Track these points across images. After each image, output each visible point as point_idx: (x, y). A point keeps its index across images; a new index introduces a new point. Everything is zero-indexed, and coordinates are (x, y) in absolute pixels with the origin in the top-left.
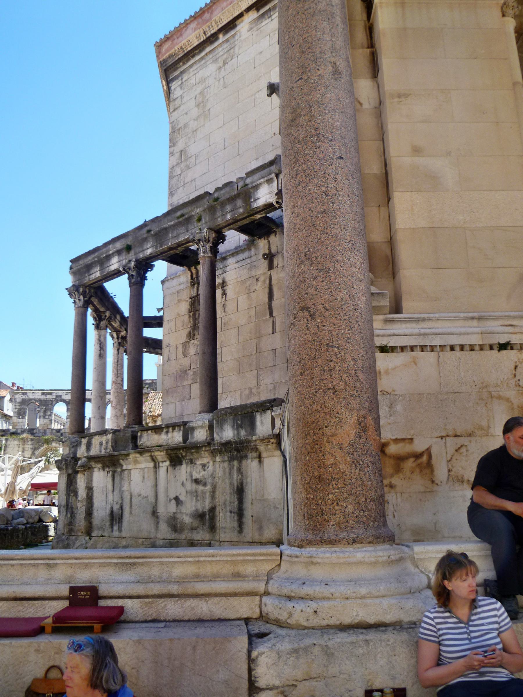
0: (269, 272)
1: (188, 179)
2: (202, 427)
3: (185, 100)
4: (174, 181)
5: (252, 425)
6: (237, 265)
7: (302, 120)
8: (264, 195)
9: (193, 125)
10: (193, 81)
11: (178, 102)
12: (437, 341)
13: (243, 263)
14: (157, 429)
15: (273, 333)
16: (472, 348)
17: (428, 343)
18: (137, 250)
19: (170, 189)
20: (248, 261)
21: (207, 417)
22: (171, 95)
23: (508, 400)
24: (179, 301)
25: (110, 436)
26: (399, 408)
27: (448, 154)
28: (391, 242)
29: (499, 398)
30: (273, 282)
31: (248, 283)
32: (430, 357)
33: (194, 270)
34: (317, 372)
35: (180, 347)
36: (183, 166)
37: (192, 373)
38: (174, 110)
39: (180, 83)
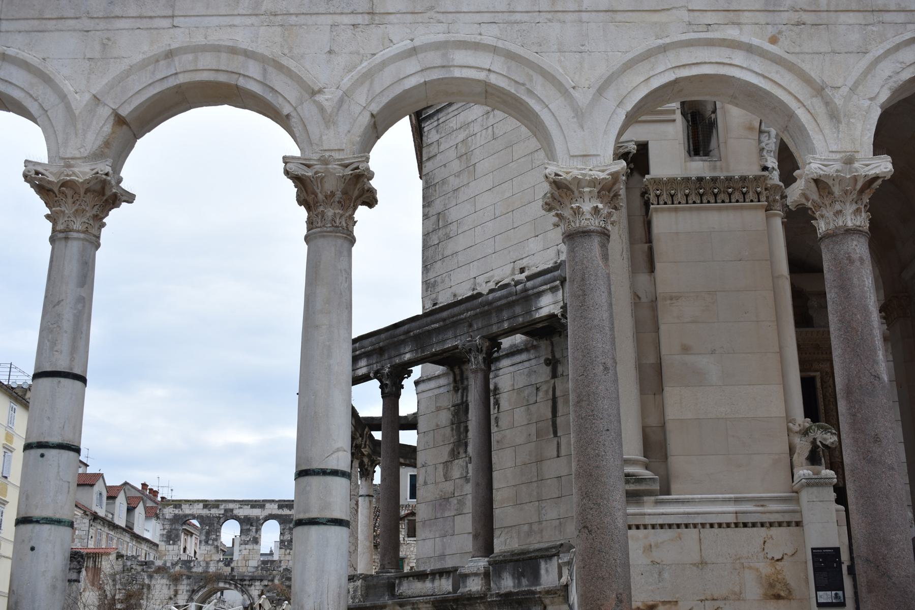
0: (553, 381)
1: (448, 252)
2: (476, 574)
3: (442, 148)
4: (430, 252)
5: (535, 577)
6: (512, 369)
7: (584, 404)
8: (548, 305)
9: (454, 182)
10: (454, 123)
11: (433, 150)
12: (699, 520)
13: (520, 366)
14: (421, 576)
15: (558, 456)
16: (728, 525)
17: (691, 521)
18: (393, 353)
19: (424, 262)
20: (527, 364)
21: (482, 563)
22: (424, 138)
23: (757, 570)
24: (438, 409)
25: (359, 583)
26: (666, 575)
27: (713, 352)
28: (663, 426)
29: (750, 568)
30: (558, 393)
31: (526, 392)
32: (693, 532)
33: (457, 371)
34: (593, 567)
35: (441, 468)
36: (441, 233)
37: (456, 502)
38: (429, 159)
39: (435, 124)
